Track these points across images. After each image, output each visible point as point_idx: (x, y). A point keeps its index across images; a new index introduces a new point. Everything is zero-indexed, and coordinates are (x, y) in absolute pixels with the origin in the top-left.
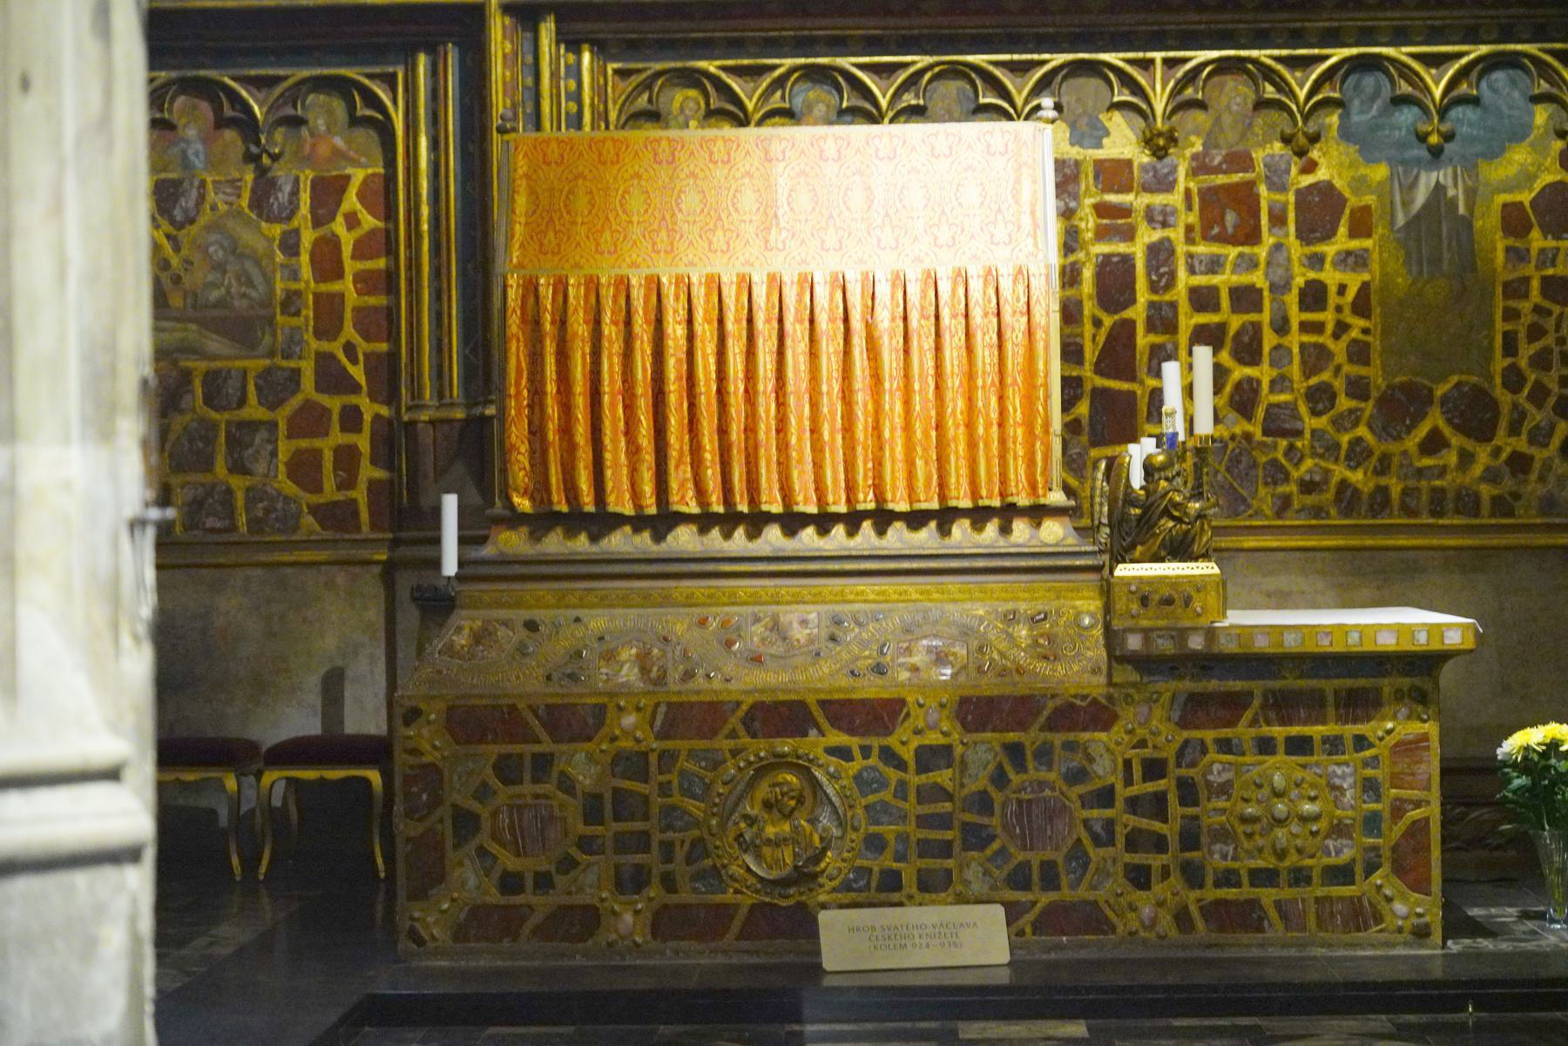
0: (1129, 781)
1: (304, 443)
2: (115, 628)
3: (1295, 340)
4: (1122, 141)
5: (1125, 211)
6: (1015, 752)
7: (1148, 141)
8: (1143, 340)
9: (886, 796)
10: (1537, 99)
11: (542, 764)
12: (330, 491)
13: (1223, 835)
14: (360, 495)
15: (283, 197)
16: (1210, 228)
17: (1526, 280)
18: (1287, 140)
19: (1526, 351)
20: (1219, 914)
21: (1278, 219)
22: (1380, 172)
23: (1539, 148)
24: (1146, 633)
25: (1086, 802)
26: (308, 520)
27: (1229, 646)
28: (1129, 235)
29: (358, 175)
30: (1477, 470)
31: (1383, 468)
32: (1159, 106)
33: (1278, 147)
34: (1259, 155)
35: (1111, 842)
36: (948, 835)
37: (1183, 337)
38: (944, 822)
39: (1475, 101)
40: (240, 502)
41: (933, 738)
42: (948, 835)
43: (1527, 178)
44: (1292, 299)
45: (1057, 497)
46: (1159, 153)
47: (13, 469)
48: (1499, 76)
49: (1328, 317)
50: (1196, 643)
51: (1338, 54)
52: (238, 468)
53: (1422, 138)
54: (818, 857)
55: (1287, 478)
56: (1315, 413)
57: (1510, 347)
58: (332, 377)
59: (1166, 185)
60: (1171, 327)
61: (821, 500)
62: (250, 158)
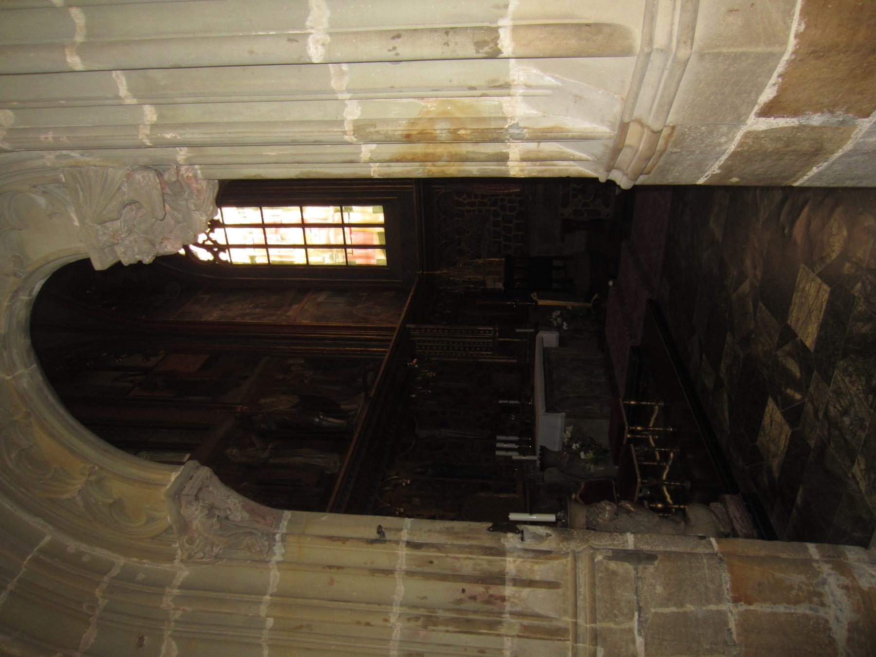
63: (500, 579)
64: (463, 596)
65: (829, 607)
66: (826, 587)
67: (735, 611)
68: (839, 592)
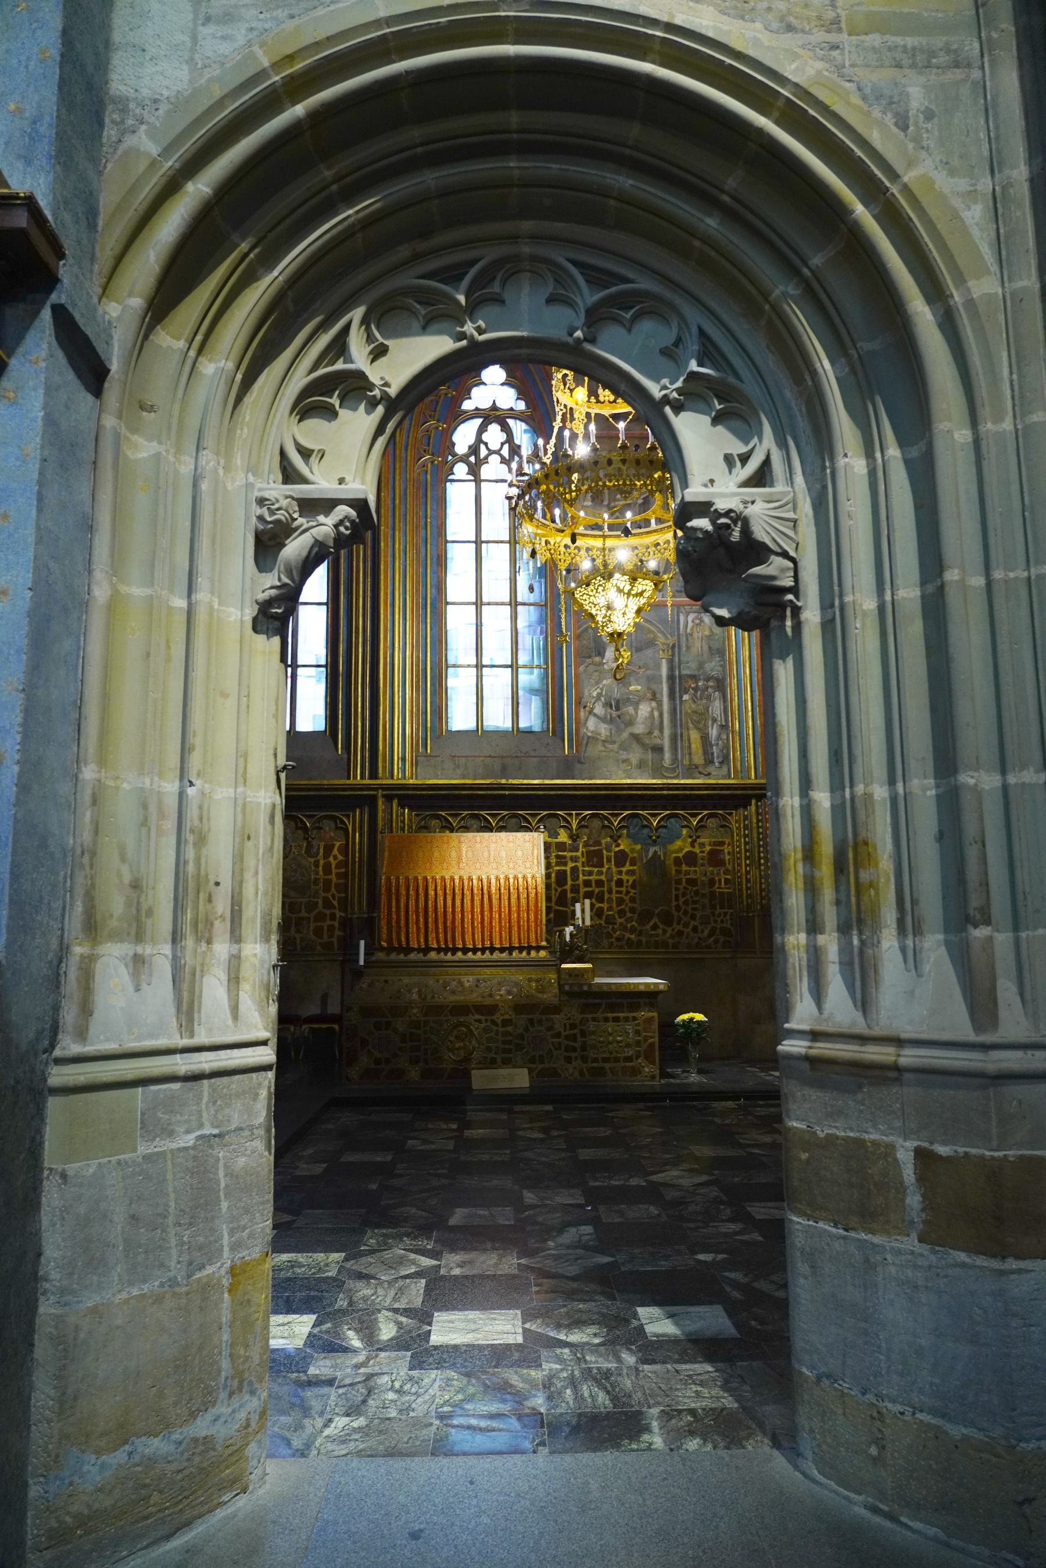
0: (565, 1030)
1: (318, 924)
2: (268, 999)
3: (614, 896)
4: (563, 837)
5: (564, 857)
6: (531, 1021)
7: (571, 837)
8: (569, 895)
9: (493, 1034)
10: (683, 827)
11: (388, 1024)
12: (325, 939)
14: (335, 940)
15: (315, 850)
16: (588, 863)
17: (681, 879)
18: (611, 837)
19: (682, 900)
21: (609, 860)
22: (639, 847)
23: (684, 841)
24: (571, 985)
25: (552, 1037)
26: (319, 948)
27: (596, 990)
28: (565, 864)
29: (338, 844)
30: (668, 935)
31: (640, 934)
32: (574, 827)
33: (609, 839)
34: (603, 841)
35: (560, 1049)
37: (581, 895)
39: (665, 827)
40: (298, 942)
41: (507, 1017)
43: (681, 849)
44: (613, 883)
45: (544, 943)
46: (574, 841)
47: (240, 951)
49: (624, 889)
50: (585, 988)
51: (626, 813)
52: (298, 931)
53: (651, 837)
55: (612, 937)
56: (620, 918)
57: (677, 899)
58: (327, 904)
59: (577, 851)
60: (578, 892)
61: (474, 944)
62: (306, 839)
63: (236, 937)
64: (212, 883)
65: (229, 1405)
66: (247, 1397)
67: (223, 1272)
68: (242, 1415)
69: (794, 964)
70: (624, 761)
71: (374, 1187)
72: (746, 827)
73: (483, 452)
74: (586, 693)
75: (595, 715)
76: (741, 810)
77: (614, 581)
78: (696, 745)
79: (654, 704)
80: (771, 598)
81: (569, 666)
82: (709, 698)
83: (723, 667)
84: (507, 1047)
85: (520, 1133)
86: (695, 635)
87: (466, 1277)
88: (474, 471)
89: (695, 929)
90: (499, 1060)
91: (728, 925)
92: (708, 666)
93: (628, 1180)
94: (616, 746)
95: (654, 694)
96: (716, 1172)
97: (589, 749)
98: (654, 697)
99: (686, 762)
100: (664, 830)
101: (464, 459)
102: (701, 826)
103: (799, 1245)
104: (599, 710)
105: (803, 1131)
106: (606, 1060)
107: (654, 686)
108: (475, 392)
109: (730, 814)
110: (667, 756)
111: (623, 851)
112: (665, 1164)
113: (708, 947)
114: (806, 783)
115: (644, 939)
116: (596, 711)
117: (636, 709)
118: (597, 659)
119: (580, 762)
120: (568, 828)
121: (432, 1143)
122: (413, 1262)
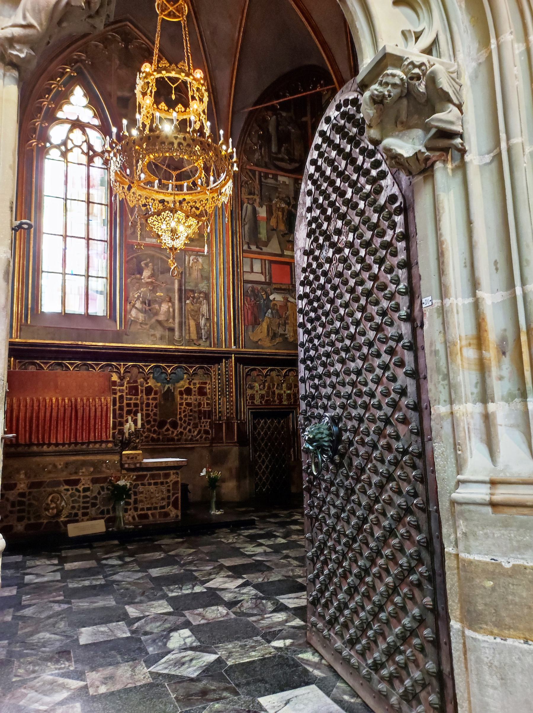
4: (115, 378)
5: (115, 389)
7: (120, 378)
9: (76, 498)
10: (185, 373)
13: (142, 501)
16: (129, 393)
18: (144, 378)
19: (183, 414)
20: (141, 517)
21: (142, 392)
22: (159, 384)
24: (129, 464)
27: (144, 466)
28: (115, 394)
32: (122, 372)
34: (139, 381)
36: (88, 505)
37: (125, 412)
38: (87, 502)
41: (86, 486)
42: (88, 505)
44: (144, 405)
45: (111, 439)
48: (179, 369)
49: (150, 408)
50: (138, 465)
51: (153, 365)
53: (166, 379)
54: (61, 511)
59: (123, 385)
61: (64, 441)
69: (464, 428)
70: (152, 335)
71: (9, 618)
72: (219, 374)
73: (70, 145)
74: (131, 294)
75: (136, 308)
76: (217, 365)
77: (176, 215)
78: (193, 329)
79: (170, 304)
80: (442, 143)
81: (121, 279)
82: (200, 303)
83: (209, 287)
84: (86, 505)
85: (104, 562)
86: (194, 267)
87: (112, 693)
88: (64, 155)
89: (190, 431)
90: (80, 513)
91: (207, 428)
92: (201, 285)
93: (193, 589)
94: (148, 326)
95: (170, 299)
96: (244, 576)
97: (132, 327)
98: (170, 300)
99: (187, 338)
100: (174, 375)
101: (58, 147)
102: (195, 374)
103: (486, 659)
104: (138, 305)
105: (487, 563)
106: (149, 509)
107: (170, 294)
108: (66, 107)
109: (210, 367)
110: (177, 333)
111: (150, 387)
112: (210, 574)
113: (197, 440)
114: (474, 284)
115: (161, 437)
116: (136, 306)
117: (160, 306)
118: (138, 276)
119: (126, 334)
120: (118, 373)
121: (43, 576)
122: (63, 686)
